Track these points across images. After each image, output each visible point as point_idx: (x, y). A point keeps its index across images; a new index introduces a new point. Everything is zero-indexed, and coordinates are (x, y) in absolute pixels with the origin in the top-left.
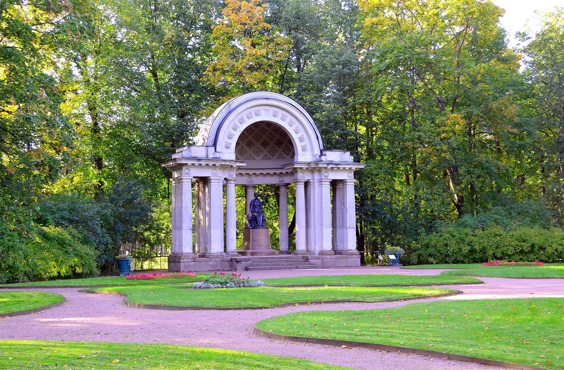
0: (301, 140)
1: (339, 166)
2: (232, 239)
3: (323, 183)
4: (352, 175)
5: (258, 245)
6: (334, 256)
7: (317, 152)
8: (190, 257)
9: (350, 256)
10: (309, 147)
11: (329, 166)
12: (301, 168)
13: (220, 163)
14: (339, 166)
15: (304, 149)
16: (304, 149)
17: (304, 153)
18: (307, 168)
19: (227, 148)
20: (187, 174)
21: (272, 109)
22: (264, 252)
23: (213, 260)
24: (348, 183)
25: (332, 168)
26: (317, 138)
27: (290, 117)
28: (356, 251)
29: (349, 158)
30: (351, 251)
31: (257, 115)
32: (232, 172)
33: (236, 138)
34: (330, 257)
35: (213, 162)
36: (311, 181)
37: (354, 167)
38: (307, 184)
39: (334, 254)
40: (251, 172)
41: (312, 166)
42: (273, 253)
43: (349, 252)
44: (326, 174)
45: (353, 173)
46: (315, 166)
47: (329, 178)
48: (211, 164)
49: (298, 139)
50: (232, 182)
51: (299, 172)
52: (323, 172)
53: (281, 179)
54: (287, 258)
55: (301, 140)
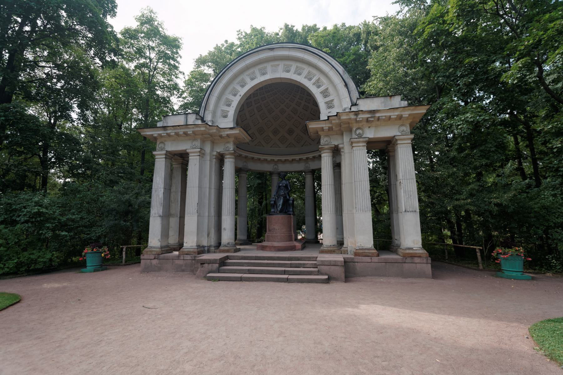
0: (325, 93)
1: (377, 115)
2: (225, 229)
3: (354, 145)
4: (407, 129)
6: (375, 259)
7: (347, 104)
8: (154, 253)
9: (408, 260)
10: (336, 103)
12: (322, 129)
13: (192, 130)
14: (377, 115)
15: (330, 105)
16: (330, 105)
17: (330, 110)
18: (330, 129)
19: (225, 116)
20: (162, 149)
21: (281, 64)
22: (275, 247)
23: (182, 258)
24: (399, 142)
25: (367, 120)
26: (346, 85)
27: (307, 69)
28: (421, 252)
29: (400, 104)
30: (411, 251)
31: (264, 74)
32: (228, 145)
33: (235, 104)
34: (368, 259)
35: (183, 128)
36: (340, 146)
37: (406, 114)
38: (336, 151)
39: (375, 255)
40: (304, 157)
41: (333, 122)
42: (293, 248)
43: (408, 251)
44: (359, 131)
45: (408, 126)
46: (337, 121)
47: (363, 136)
48: (181, 132)
50: (228, 156)
51: (322, 137)
52: (354, 129)
55: (325, 93)
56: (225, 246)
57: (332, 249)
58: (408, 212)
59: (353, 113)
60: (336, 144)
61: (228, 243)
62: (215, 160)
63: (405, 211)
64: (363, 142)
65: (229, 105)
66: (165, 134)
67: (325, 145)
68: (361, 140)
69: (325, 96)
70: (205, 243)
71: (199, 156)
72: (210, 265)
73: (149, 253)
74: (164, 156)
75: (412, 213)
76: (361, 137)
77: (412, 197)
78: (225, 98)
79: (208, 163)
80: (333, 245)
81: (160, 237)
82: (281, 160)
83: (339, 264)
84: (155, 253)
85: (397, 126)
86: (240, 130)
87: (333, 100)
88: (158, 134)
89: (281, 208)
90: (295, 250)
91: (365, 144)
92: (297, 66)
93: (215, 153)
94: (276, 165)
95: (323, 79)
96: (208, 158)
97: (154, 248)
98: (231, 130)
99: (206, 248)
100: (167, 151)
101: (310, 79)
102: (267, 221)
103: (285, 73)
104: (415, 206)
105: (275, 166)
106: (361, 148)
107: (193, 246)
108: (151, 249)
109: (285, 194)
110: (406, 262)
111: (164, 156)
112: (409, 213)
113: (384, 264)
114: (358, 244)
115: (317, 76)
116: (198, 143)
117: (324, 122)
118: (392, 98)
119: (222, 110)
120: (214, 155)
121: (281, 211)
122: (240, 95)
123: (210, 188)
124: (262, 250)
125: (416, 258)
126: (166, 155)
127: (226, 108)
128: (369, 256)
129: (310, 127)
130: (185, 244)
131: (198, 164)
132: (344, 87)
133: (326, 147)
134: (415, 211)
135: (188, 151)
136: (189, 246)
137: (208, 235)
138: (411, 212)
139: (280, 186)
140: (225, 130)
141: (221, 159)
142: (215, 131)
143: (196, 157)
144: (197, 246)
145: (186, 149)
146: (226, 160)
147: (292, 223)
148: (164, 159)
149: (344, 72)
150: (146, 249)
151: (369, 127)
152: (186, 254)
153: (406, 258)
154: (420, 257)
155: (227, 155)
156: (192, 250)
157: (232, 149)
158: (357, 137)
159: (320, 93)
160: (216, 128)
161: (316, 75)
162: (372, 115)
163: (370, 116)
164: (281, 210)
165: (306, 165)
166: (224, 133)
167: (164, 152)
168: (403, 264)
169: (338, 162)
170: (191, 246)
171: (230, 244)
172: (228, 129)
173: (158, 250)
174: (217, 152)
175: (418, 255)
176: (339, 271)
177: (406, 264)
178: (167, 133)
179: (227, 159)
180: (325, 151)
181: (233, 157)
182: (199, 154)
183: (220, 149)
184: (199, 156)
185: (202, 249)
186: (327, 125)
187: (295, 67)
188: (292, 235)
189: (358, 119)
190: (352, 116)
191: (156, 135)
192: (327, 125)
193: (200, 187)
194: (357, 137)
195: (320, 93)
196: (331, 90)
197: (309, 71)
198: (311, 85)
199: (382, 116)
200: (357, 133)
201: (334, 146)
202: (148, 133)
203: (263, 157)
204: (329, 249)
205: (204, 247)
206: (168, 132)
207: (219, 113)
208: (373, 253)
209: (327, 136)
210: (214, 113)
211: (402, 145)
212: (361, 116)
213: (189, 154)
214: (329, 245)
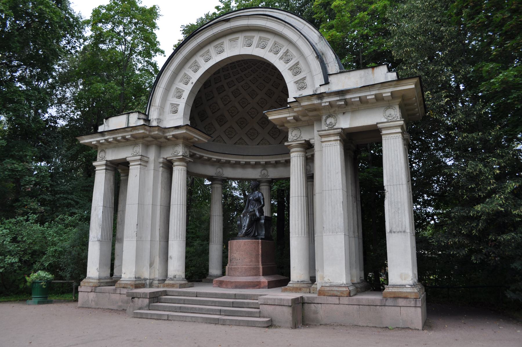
0: (295, 70)
1: (348, 97)
2: (171, 257)
3: (324, 139)
4: (395, 113)
9: (390, 302)
10: (308, 81)
11: (324, 101)
19: (175, 112)
21: (241, 37)
22: (232, 282)
23: (118, 291)
24: (384, 132)
27: (272, 40)
29: (386, 77)
34: (335, 300)
35: (121, 133)
36: (312, 141)
44: (330, 120)
47: (335, 127)
49: (290, 73)
52: (324, 118)
54: (235, 296)
56: (171, 279)
57: (298, 286)
58: (394, 232)
59: (315, 97)
60: (307, 139)
61: (175, 277)
62: (161, 168)
63: (391, 232)
64: (335, 135)
65: (179, 97)
66: (103, 141)
67: (293, 141)
68: (332, 132)
69: (296, 74)
70: (146, 274)
71: (140, 164)
72: (140, 299)
73: (86, 284)
74: (104, 167)
75: (400, 234)
76: (332, 129)
77: (400, 211)
78: (175, 88)
79: (152, 172)
80: (301, 282)
81: (98, 266)
83: (285, 303)
84: (91, 284)
85: (382, 110)
87: (305, 77)
88: (97, 141)
89: (247, 230)
90: (260, 288)
91: (338, 138)
92: (260, 37)
93: (161, 160)
94: (264, 170)
95: (292, 51)
96: (151, 166)
97: (92, 278)
99: (148, 282)
100: (107, 161)
101: (276, 53)
102: (229, 248)
103: (245, 47)
104: (404, 224)
105: (264, 172)
106: (332, 143)
107: (131, 278)
108: (89, 280)
110: (387, 304)
111: (104, 167)
112: (396, 234)
113: (357, 307)
114: (326, 280)
115: (285, 47)
116: (139, 149)
118: (375, 68)
119: (171, 104)
120: (160, 163)
121: (247, 235)
122: (192, 83)
123: (154, 205)
125: (400, 300)
126: (106, 165)
127: (175, 101)
128: (336, 296)
130: (123, 276)
131: (138, 175)
132: (316, 59)
133: (294, 143)
134: (404, 232)
135: (128, 159)
136: (128, 277)
137: (151, 265)
138: (398, 232)
140: (169, 130)
141: (169, 166)
142: (156, 132)
143: (137, 166)
144: (136, 278)
145: (125, 159)
146: (175, 169)
147: (260, 251)
148: (105, 171)
149: (320, 37)
150: (84, 280)
151: (344, 113)
152: (123, 288)
153: (386, 300)
154: (406, 298)
155: (176, 161)
156: (129, 282)
157: (181, 154)
158: (327, 128)
159: (289, 69)
160: (157, 128)
161: (284, 46)
162: (341, 98)
163: (338, 98)
166: (170, 135)
167: (104, 162)
168: (383, 307)
170: (129, 278)
171: (177, 277)
172: (172, 129)
173: (96, 281)
174: (163, 158)
175: (403, 295)
176: (286, 313)
177: (386, 307)
178: (105, 139)
182: (139, 163)
183: (168, 154)
184: (140, 164)
185: (143, 282)
186: (291, 115)
187: (258, 38)
188: (259, 268)
189: (323, 104)
190: (316, 102)
191: (94, 143)
192: (291, 115)
193: (141, 204)
194: (327, 128)
195: (289, 69)
196: (302, 65)
197: (275, 41)
198: (278, 60)
199: (354, 98)
200: (328, 122)
201: (303, 142)
202: (86, 141)
203: (243, 160)
205: (145, 279)
206: (106, 138)
207: (168, 108)
208: (342, 292)
209: (296, 128)
210: (162, 108)
211: (388, 136)
212: (326, 102)
213: (129, 164)
214: (296, 281)
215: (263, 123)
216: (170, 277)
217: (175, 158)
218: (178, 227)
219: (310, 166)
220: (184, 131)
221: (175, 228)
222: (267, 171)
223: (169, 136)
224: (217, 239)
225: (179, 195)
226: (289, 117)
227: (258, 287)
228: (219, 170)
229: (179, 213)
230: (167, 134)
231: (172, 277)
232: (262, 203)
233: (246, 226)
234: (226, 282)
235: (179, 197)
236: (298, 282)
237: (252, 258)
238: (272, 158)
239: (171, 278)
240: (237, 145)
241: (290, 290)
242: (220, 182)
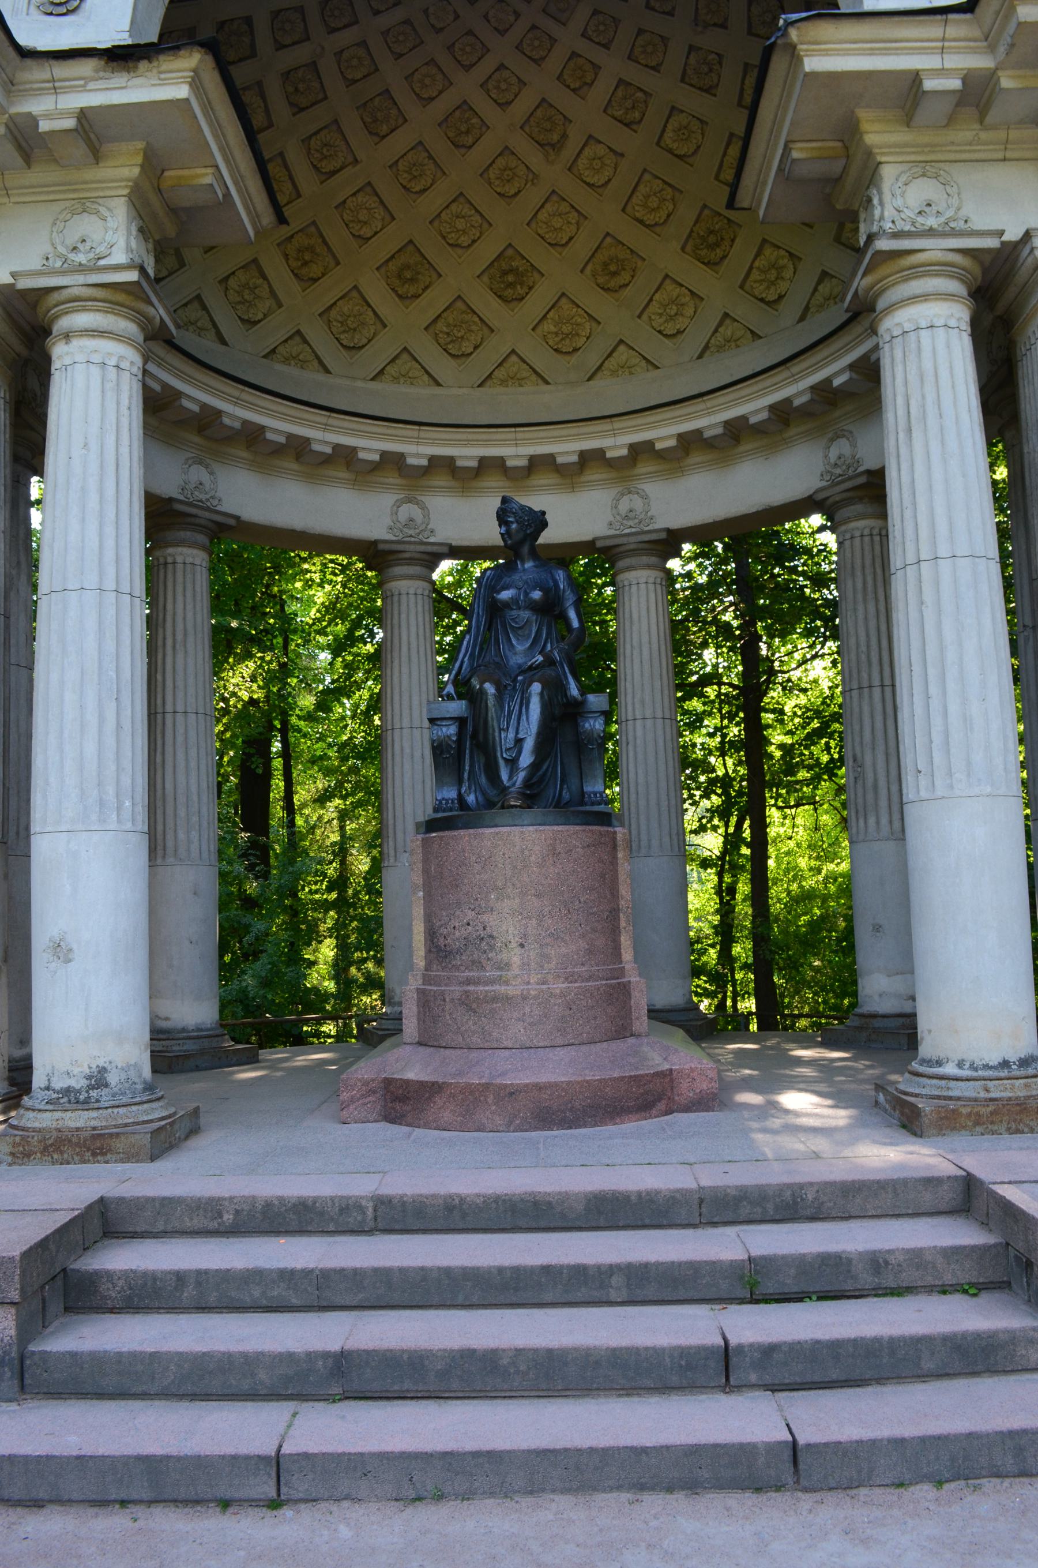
2: (61, 951)
5: (467, 1003)
22: (512, 1093)
32: (87, 226)
51: (889, 173)
53: (840, 448)
61: (98, 1080)
82: (451, 460)
86: (196, 83)
89: (534, 767)
90: (669, 1112)
94: (409, 500)
98: (120, 79)
109: (550, 662)
117: (932, 29)
124: (391, 1117)
129: (812, 64)
133: (935, 249)
139: (507, 605)
146: (61, 353)
155: (79, 303)
164: (527, 783)
165: (624, 506)
169: (870, 464)
171: (113, 1079)
172: (86, 67)
179: (76, 343)
180: (917, 286)
181: (127, 326)
204: (998, 1091)
214: (994, 1059)
215: (408, 275)
216: (58, 1084)
217: (81, 279)
218: (110, 741)
219: (645, 497)
220: (182, 92)
221: (90, 748)
222: (423, 507)
223: (48, 116)
224: (194, 834)
225: (110, 530)
226: (941, 73)
227: (662, 1106)
228: (198, 474)
229: (110, 646)
230: (38, 106)
231: (78, 1083)
232: (575, 624)
233: (529, 744)
234: (469, 1090)
235: (110, 543)
236: (1005, 1064)
237: (594, 930)
238: (468, 443)
239: (67, 1091)
240: (279, 367)
241: (977, 1123)
242: (202, 539)
